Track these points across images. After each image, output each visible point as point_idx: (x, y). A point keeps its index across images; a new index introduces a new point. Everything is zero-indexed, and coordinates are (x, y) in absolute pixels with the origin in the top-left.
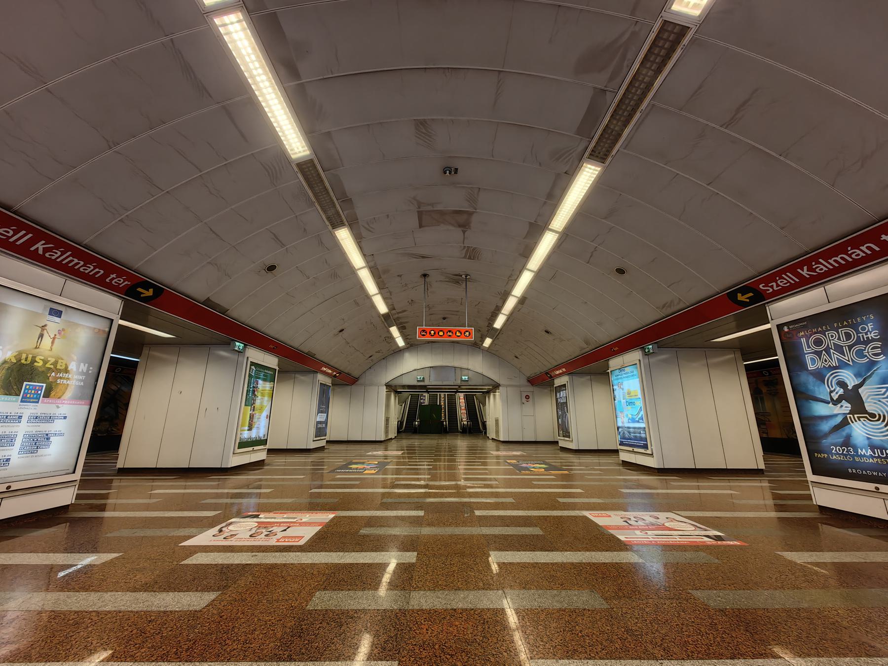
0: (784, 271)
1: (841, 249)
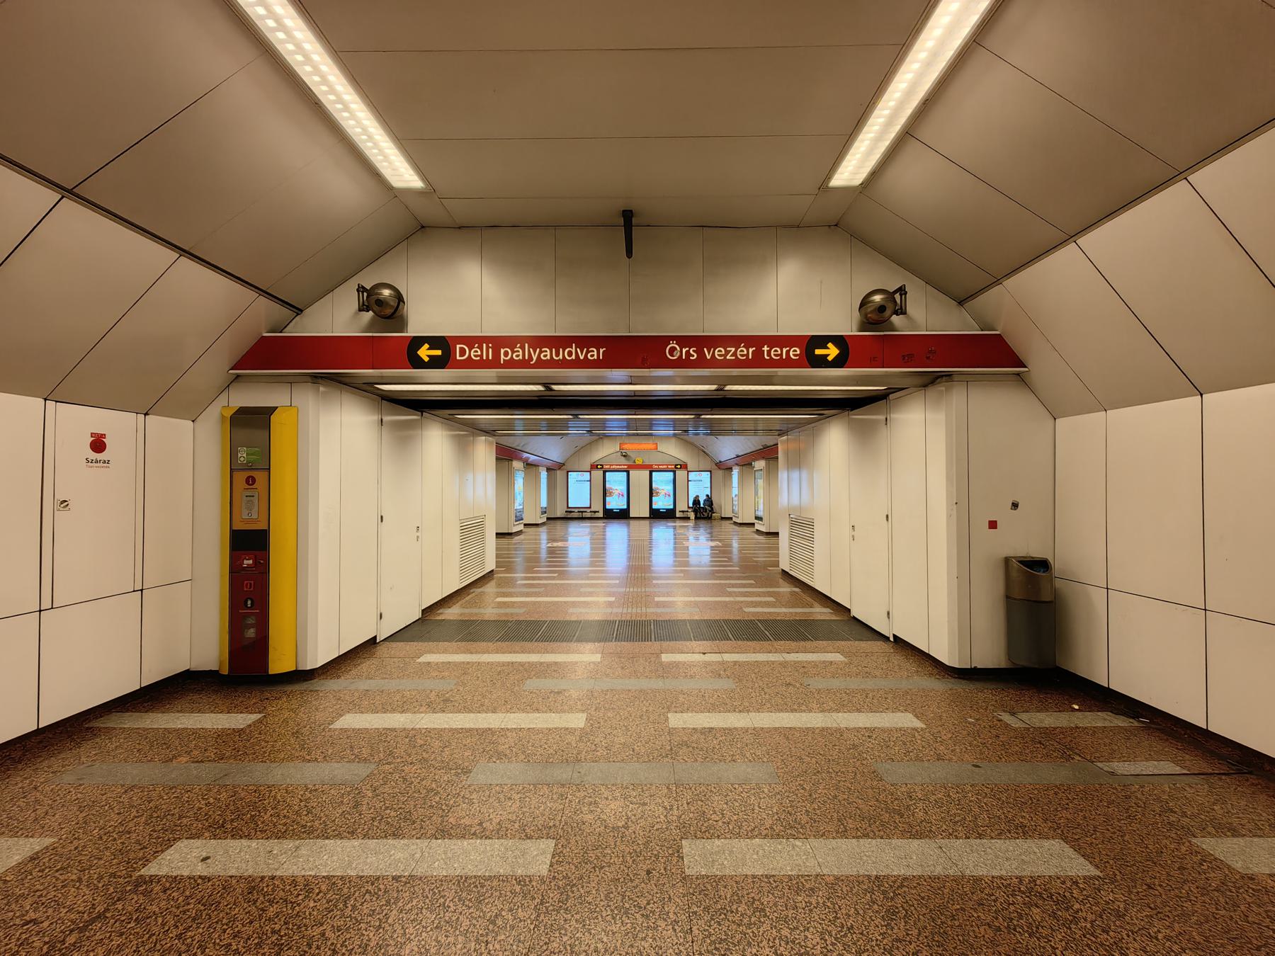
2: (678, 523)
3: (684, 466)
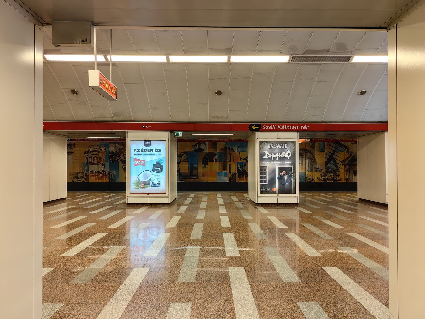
0: (274, 125)
1: (292, 125)
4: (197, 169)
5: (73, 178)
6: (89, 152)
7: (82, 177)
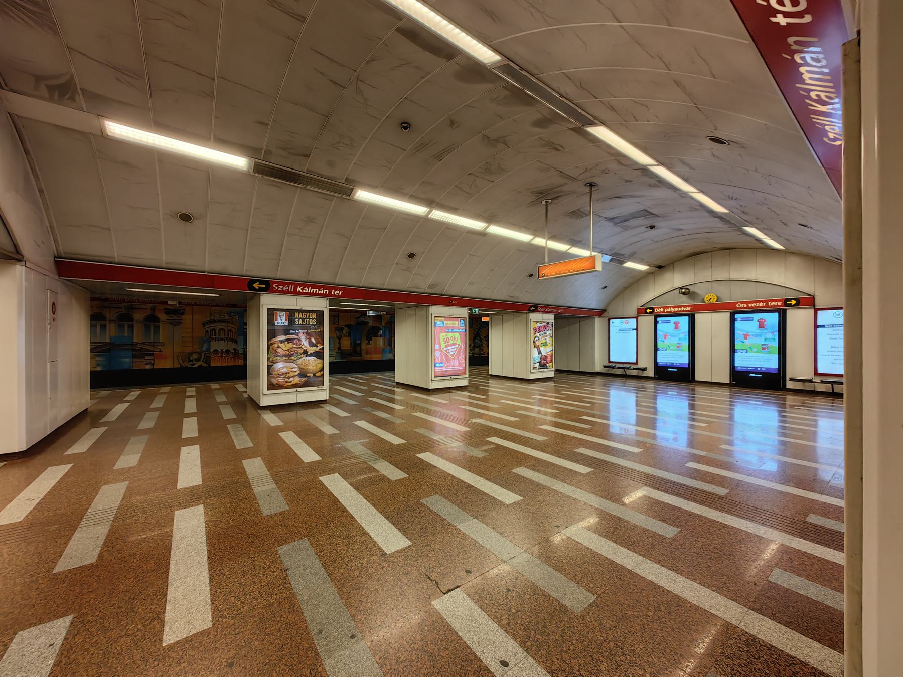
2: (790, 399)
3: (807, 302)
4: (360, 344)
5: (181, 361)
6: (211, 322)
7: (198, 360)
